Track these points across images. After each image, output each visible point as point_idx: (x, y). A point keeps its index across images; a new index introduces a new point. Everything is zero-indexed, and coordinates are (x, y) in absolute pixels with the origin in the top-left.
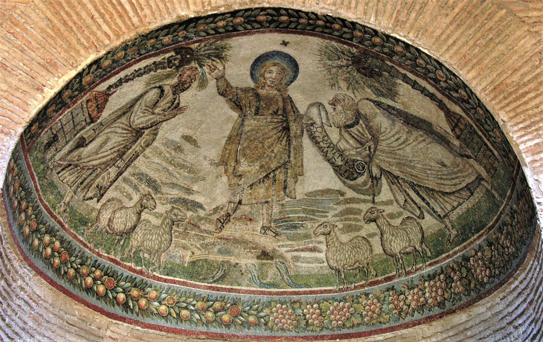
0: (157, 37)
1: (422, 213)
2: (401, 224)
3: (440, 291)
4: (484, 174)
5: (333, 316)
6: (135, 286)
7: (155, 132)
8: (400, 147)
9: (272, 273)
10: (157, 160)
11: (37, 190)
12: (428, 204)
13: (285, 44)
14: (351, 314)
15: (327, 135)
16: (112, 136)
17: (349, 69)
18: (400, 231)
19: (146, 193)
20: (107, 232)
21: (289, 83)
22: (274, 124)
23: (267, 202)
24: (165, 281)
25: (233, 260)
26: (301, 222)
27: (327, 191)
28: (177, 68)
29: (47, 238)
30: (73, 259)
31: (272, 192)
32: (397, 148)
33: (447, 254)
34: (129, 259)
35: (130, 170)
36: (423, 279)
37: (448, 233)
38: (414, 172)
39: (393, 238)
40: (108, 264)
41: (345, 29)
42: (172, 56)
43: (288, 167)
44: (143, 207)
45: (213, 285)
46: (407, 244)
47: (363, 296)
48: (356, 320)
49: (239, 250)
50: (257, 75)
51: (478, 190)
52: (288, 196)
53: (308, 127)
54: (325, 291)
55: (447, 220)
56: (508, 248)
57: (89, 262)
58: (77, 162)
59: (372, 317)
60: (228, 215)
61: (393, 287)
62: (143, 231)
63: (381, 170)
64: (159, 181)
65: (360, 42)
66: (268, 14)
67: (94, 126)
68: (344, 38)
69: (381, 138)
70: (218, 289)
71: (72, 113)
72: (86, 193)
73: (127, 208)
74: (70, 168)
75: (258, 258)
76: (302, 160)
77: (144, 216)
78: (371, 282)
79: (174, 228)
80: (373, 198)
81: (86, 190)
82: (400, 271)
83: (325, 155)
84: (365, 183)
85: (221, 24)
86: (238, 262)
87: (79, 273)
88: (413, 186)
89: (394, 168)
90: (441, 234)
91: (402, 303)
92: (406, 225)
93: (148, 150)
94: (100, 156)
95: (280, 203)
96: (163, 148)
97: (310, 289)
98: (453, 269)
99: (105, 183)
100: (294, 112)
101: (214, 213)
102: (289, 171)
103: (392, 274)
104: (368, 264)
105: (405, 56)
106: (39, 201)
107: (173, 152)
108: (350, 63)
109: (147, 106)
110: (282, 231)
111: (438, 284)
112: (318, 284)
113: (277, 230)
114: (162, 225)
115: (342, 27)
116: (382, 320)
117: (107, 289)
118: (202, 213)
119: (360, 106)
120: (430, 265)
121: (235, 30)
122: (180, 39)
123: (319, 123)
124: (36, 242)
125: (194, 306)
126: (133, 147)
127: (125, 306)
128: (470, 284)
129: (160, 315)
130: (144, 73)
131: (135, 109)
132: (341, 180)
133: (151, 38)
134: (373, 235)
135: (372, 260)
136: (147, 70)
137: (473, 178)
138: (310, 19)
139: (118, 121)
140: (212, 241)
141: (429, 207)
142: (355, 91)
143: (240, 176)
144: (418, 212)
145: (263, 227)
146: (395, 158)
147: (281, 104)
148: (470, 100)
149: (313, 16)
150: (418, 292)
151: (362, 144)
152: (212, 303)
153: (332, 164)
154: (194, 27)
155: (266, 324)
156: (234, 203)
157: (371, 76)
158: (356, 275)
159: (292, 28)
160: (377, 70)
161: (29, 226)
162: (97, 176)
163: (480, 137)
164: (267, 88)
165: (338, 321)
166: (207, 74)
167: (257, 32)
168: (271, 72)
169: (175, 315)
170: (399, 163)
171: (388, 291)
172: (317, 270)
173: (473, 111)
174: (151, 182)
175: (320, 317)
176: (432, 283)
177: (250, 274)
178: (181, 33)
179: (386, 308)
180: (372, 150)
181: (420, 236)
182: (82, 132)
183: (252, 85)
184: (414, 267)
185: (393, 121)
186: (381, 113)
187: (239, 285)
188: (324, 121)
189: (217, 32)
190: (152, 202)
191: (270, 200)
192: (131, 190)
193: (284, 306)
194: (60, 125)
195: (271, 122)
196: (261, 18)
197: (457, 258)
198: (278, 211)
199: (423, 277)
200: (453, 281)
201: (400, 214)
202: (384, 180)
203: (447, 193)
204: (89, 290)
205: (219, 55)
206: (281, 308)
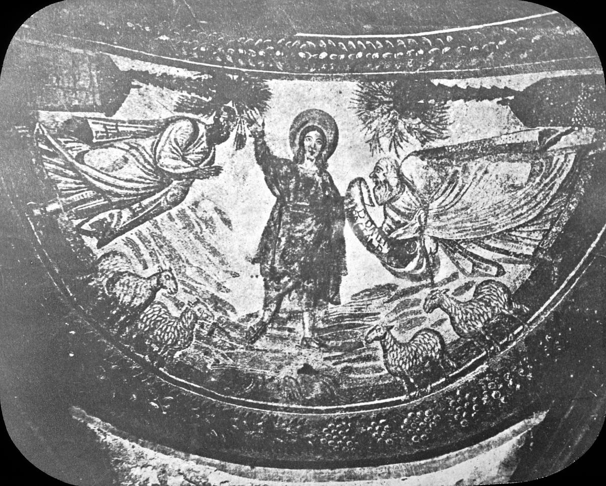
1: (500, 267)
2: (474, 296)
19: (168, 268)
35: (147, 224)
63: (436, 240)
84: (419, 266)
88: (478, 242)
89: (452, 231)
92: (481, 293)
94: (111, 180)
118: (233, 318)
131: (163, 139)
134: (441, 322)
136: (179, 85)
142: (398, 148)
162: (104, 208)
180: (423, 220)
182: (89, 115)
187: (277, 401)
190: (172, 282)
202: (441, 253)
206: (335, 428)
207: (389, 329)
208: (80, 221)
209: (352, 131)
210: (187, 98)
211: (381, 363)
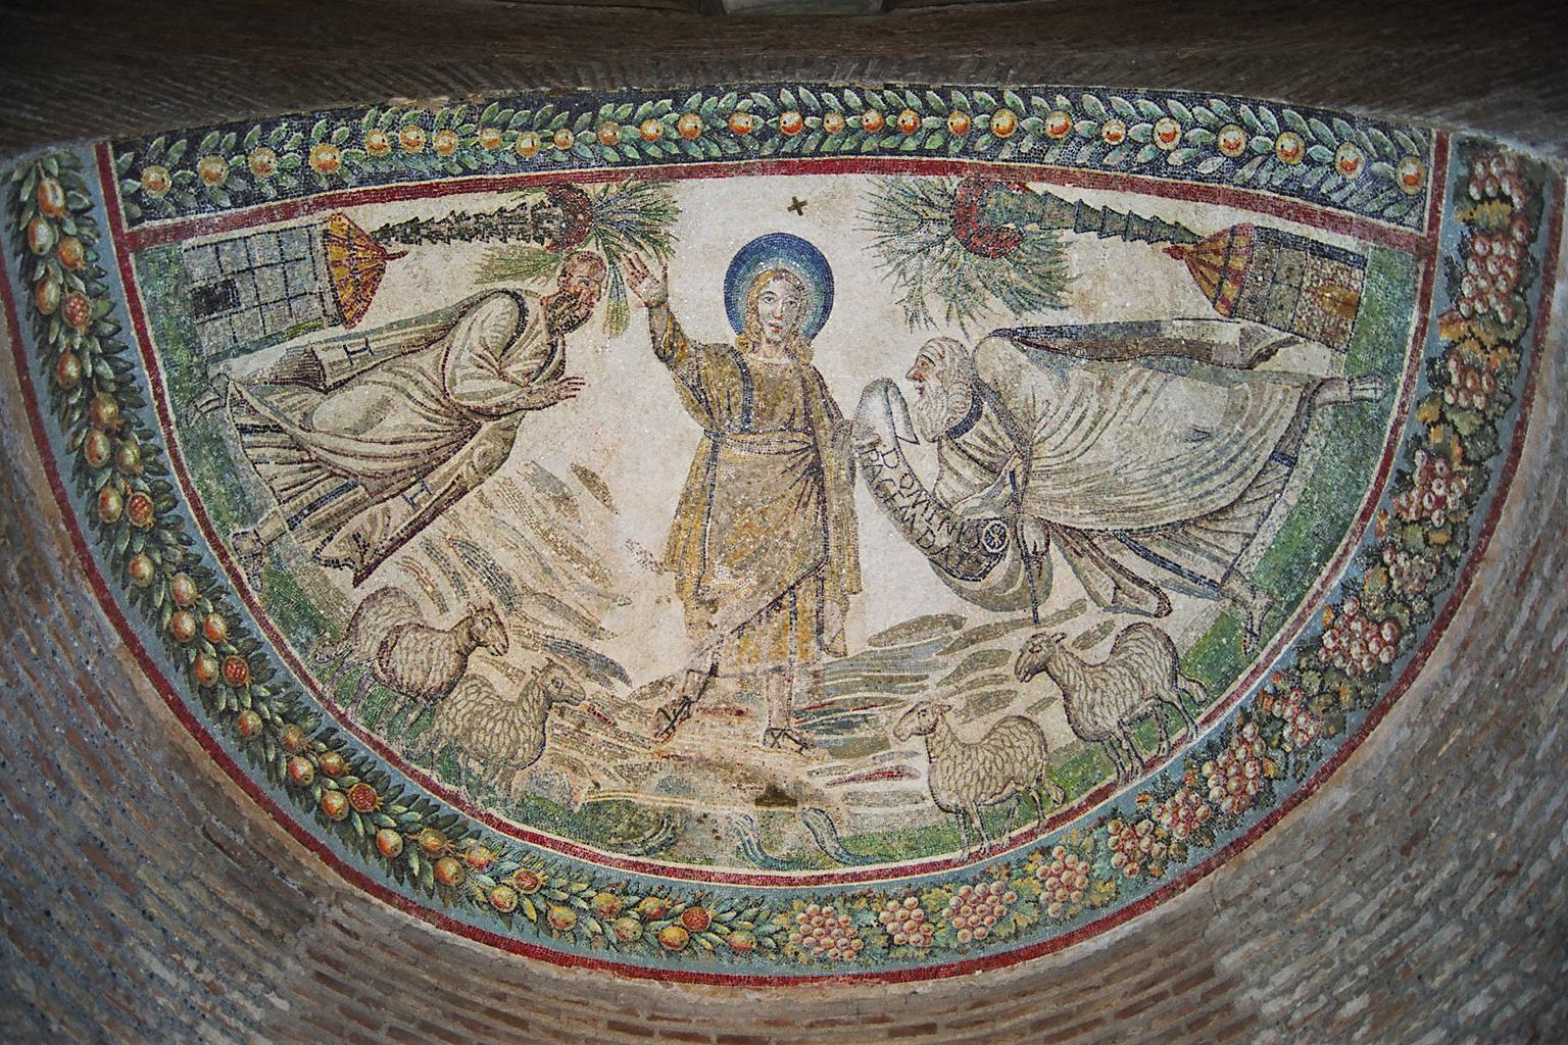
0: (504, 127)
1: (1163, 598)
6: (433, 825)
7: (509, 435)
8: (1087, 443)
9: (792, 834)
10: (510, 517)
13: (797, 206)
15: (911, 473)
17: (947, 250)
18: (1113, 671)
19: (486, 605)
20: (375, 675)
21: (812, 331)
22: (786, 457)
23: (778, 670)
24: (518, 833)
25: (696, 807)
27: (923, 623)
29: (186, 587)
30: (264, 692)
31: (790, 642)
32: (1080, 449)
36: (1195, 760)
38: (1130, 501)
39: (1098, 696)
40: (365, 751)
41: (930, 121)
43: (825, 575)
45: (641, 859)
46: (1136, 696)
48: (1026, 916)
50: (741, 308)
52: (827, 650)
53: (865, 457)
54: (934, 866)
55: (1234, 584)
57: (310, 723)
58: (299, 432)
59: (1067, 902)
60: (687, 701)
61: (1115, 810)
62: (472, 705)
63: (1046, 525)
64: (516, 582)
65: (964, 152)
67: (348, 337)
68: (928, 153)
70: (656, 871)
74: (280, 438)
75: (759, 802)
76: (856, 552)
77: (477, 663)
79: (553, 716)
80: (1035, 612)
83: (907, 525)
84: (1010, 580)
85: (650, 128)
87: (275, 734)
88: (1127, 539)
89: (1077, 510)
90: (1224, 625)
91: (1145, 842)
94: (365, 448)
95: (810, 669)
96: (527, 489)
97: (894, 865)
98: (1277, 694)
100: (830, 416)
101: (654, 694)
103: (1106, 782)
104: (1039, 780)
107: (552, 509)
109: (487, 348)
110: (816, 738)
111: (1241, 754)
112: (912, 849)
113: (805, 735)
114: (520, 701)
117: (351, 809)
118: (622, 691)
119: (978, 359)
120: (1207, 721)
122: (560, 157)
125: (588, 900)
127: (399, 864)
129: (493, 907)
130: (478, 231)
131: (457, 344)
133: (489, 124)
135: (1050, 770)
138: (848, 111)
139: (414, 359)
140: (649, 759)
141: (1181, 574)
142: (966, 319)
143: (713, 602)
144: (1154, 601)
147: (798, 396)
149: (853, 99)
150: (1186, 799)
151: (991, 469)
152: (637, 898)
153: (928, 548)
154: (591, 127)
155: (778, 950)
158: (1009, 813)
160: (1011, 226)
161: (125, 497)
162: (357, 507)
163: (1296, 243)
164: (764, 346)
167: (732, 168)
168: (771, 297)
169: (533, 915)
170: (1090, 490)
171: (1101, 825)
172: (908, 819)
174: (497, 579)
175: (925, 926)
176: (1222, 759)
177: (737, 838)
178: (560, 137)
179: (1102, 869)
181: (1168, 662)
182: (315, 336)
183: (732, 338)
184: (1165, 745)
186: (1031, 360)
187: (710, 861)
189: (647, 159)
191: (785, 663)
196: (741, 121)
198: (806, 689)
199: (1193, 757)
200: (1285, 722)
204: (297, 789)
205: (650, 230)
206: (820, 914)
207: (944, 710)
208: (317, 543)
209: (864, 277)
210: (501, 252)
211: (920, 785)
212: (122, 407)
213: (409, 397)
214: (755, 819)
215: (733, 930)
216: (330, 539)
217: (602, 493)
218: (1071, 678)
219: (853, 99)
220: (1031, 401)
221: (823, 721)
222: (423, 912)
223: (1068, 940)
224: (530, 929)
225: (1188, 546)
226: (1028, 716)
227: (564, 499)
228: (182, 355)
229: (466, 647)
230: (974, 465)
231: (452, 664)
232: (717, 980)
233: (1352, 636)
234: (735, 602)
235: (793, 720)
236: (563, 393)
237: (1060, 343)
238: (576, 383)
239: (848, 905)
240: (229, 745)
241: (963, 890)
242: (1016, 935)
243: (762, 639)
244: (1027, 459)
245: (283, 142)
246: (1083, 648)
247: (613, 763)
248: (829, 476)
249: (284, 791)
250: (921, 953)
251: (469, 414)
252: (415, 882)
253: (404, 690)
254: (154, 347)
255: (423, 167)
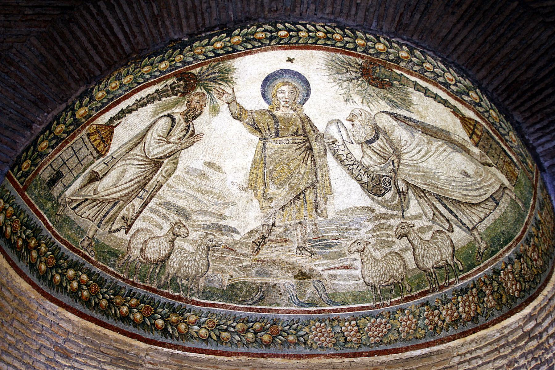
0: (152, 64)
1: (451, 225)
2: (431, 238)
3: (473, 306)
4: (507, 183)
5: (370, 333)
6: (174, 312)
7: (176, 161)
8: (422, 160)
10: (182, 189)
11: (49, 227)
12: (456, 216)
13: (290, 60)
14: (388, 330)
16: (128, 167)
17: (359, 82)
19: (177, 221)
20: (142, 262)
22: (296, 145)
23: (300, 223)
24: (205, 305)
25: (271, 281)
26: (335, 241)
28: (183, 94)
29: (71, 273)
32: (420, 161)
33: (478, 267)
34: (166, 286)
35: (154, 199)
37: (477, 245)
39: (426, 253)
40: (143, 292)
41: (346, 39)
42: (174, 83)
44: (176, 235)
45: (253, 306)
47: (399, 312)
48: (393, 336)
49: (276, 271)
50: (269, 96)
51: (503, 200)
52: (320, 216)
55: (475, 233)
56: (536, 260)
58: (94, 196)
60: (264, 237)
61: (428, 302)
63: (407, 183)
65: (364, 52)
66: (265, 31)
69: (403, 152)
70: (258, 310)
71: (72, 148)
72: (112, 226)
73: (158, 237)
74: (87, 202)
75: (296, 278)
76: (329, 179)
77: (178, 242)
78: (406, 297)
79: (210, 252)
81: (111, 223)
82: (434, 286)
84: (393, 199)
85: (218, 45)
86: (275, 282)
87: (112, 302)
88: (440, 199)
89: (419, 181)
90: (471, 245)
91: (436, 319)
93: (171, 180)
96: (187, 177)
97: (348, 307)
99: (130, 215)
100: (314, 131)
102: (318, 191)
103: (426, 289)
104: (402, 280)
105: (411, 61)
106: (53, 237)
107: (198, 181)
108: (359, 75)
109: (160, 136)
111: (471, 299)
112: (355, 301)
113: (313, 249)
115: (343, 37)
116: (418, 335)
117: (144, 317)
118: (237, 237)
120: (462, 279)
121: (235, 50)
123: (340, 141)
124: (58, 278)
125: (234, 327)
126: (155, 178)
127: (164, 331)
128: (501, 298)
129: (199, 338)
130: (148, 101)
132: (369, 196)
134: (406, 249)
136: (150, 99)
137: (497, 187)
138: (309, 31)
139: (132, 152)
141: (457, 219)
142: (370, 104)
144: (447, 226)
145: (298, 248)
146: (419, 171)
147: (299, 124)
148: (482, 103)
150: (451, 307)
152: (252, 324)
154: (191, 51)
155: (305, 343)
156: (268, 225)
157: (382, 87)
158: (391, 291)
159: (294, 43)
160: (387, 80)
161: (45, 262)
162: (120, 208)
164: (281, 108)
165: (375, 338)
166: (217, 99)
169: (215, 338)
171: (422, 306)
173: (486, 115)
174: (180, 211)
175: (358, 334)
176: (465, 297)
178: (177, 59)
181: (451, 250)
182: (92, 166)
183: (267, 107)
185: (412, 132)
187: (278, 305)
188: (345, 137)
189: (217, 55)
190: (183, 229)
191: (302, 220)
192: (160, 220)
193: (322, 325)
194: (61, 160)
195: (293, 143)
196: (260, 35)
197: (487, 271)
199: (456, 291)
200: (485, 296)
201: (429, 228)
203: (473, 204)
204: (125, 319)
205: (224, 77)
208: (110, 226)
211: (358, 273)
212: (36, 237)
213: (133, 164)
214: (295, 285)
215: (288, 334)
216: (113, 223)
217: (218, 169)
218: (416, 242)
219: (312, 28)
220: (399, 139)
221: (320, 244)
222: (176, 347)
223: (407, 349)
224: (214, 344)
225: (461, 210)
226: (399, 253)
227: (203, 175)
228: (49, 205)
229: (173, 239)
230: (377, 155)
231: (168, 247)
232: (284, 356)
233: (509, 278)
234: (280, 198)
235: (307, 244)
236: (195, 140)
237: (410, 123)
238: (200, 135)
239: (331, 323)
240: (98, 316)
241: (373, 320)
242: (390, 343)
243: (293, 210)
244: (399, 156)
245: (65, 118)
246: (421, 232)
247: (237, 266)
248: (316, 152)
249: (121, 322)
250: (356, 346)
251: (158, 160)
252: (172, 336)
253: (152, 263)
254: (40, 211)
255: (121, 92)
